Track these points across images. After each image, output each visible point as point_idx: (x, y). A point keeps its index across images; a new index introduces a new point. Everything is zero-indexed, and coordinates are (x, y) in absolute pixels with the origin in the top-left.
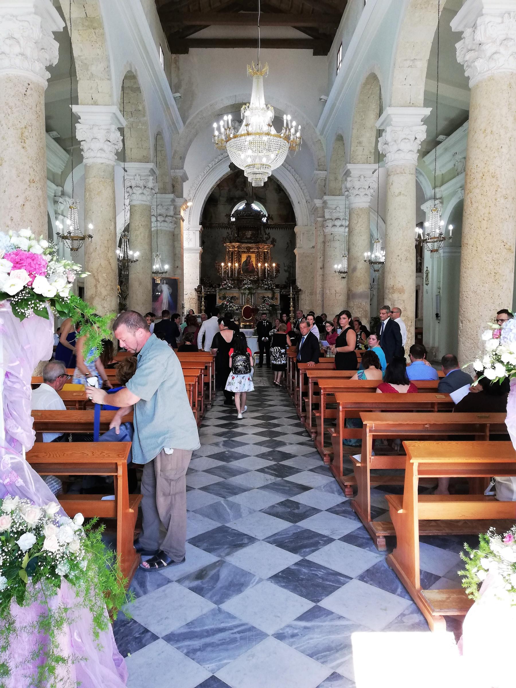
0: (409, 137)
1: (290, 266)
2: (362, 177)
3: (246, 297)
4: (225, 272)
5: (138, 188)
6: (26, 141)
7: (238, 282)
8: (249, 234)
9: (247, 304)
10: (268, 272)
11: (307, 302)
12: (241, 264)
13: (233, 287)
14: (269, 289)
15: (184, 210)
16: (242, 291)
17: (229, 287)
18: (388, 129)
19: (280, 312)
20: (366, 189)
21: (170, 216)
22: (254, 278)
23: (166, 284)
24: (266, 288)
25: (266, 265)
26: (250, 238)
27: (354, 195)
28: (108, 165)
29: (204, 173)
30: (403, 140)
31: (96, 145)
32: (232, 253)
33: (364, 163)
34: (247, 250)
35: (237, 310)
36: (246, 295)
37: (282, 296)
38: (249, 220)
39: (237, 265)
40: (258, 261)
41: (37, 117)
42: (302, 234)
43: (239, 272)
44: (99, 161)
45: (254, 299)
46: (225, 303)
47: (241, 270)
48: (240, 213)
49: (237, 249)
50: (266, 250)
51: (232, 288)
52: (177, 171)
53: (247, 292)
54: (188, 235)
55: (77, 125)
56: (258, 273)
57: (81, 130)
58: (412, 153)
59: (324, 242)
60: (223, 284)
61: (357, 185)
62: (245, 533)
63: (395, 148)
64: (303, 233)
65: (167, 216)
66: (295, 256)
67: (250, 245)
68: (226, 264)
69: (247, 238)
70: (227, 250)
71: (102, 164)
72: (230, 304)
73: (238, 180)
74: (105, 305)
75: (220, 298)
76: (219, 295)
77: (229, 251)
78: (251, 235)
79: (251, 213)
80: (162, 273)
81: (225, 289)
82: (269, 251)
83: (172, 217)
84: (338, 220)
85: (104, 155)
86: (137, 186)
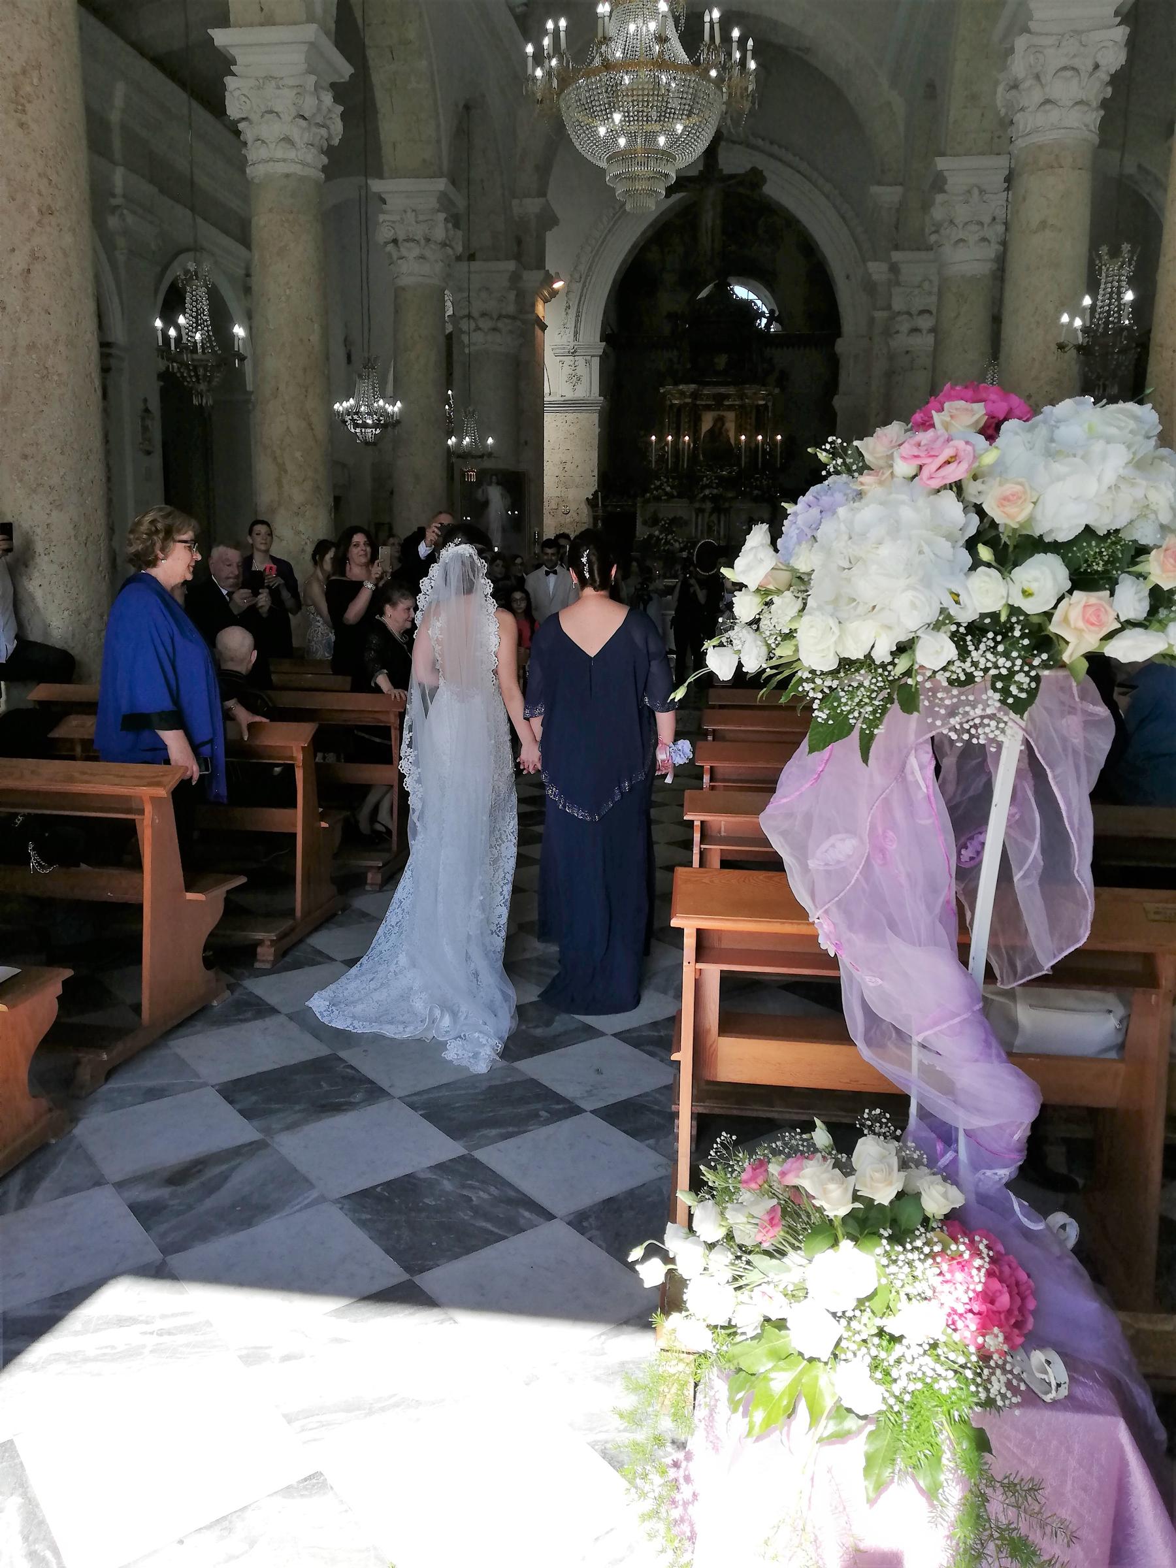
0: (1076, 62)
2: (976, 191)
3: (706, 520)
4: (662, 459)
5: (412, 244)
6: (29, 107)
7: (687, 485)
8: (721, 361)
12: (699, 438)
13: (675, 493)
15: (546, 301)
16: (697, 505)
17: (666, 494)
18: (1020, 43)
20: (986, 226)
21: (508, 316)
22: (730, 473)
23: (498, 484)
27: (952, 242)
28: (302, 179)
29: (614, 208)
30: (1059, 73)
31: (271, 130)
33: (982, 154)
35: (682, 550)
36: (707, 515)
40: (739, 431)
41: (54, 45)
44: (281, 168)
46: (657, 533)
50: (762, 402)
52: (528, 201)
54: (573, 368)
55: (228, 80)
56: (739, 457)
57: (236, 93)
58: (1086, 108)
59: (890, 374)
60: (653, 486)
61: (961, 213)
62: (372, 1076)
63: (1037, 96)
65: (500, 317)
66: (835, 414)
67: (722, 390)
68: (661, 438)
70: (668, 403)
71: (287, 176)
72: (666, 535)
74: (301, 528)
77: (672, 405)
80: (482, 457)
81: (658, 499)
82: (770, 404)
83: (514, 318)
84: (926, 316)
85: (292, 154)
86: (408, 240)
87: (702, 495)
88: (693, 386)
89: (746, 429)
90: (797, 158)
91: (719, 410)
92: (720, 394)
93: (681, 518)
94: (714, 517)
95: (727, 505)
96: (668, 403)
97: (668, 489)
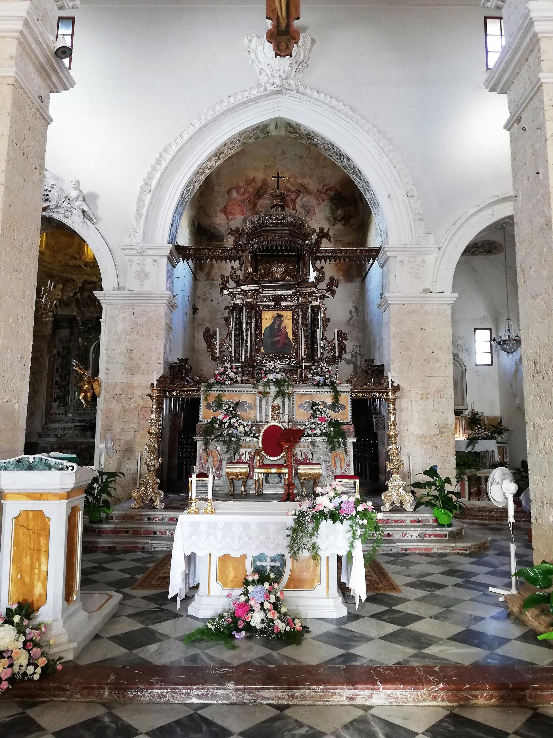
1: (356, 353)
3: (270, 404)
8: (278, 270)
9: (275, 420)
10: (320, 351)
11: (416, 416)
13: (239, 379)
14: (325, 385)
16: (261, 389)
17: (230, 379)
19: (354, 439)
22: (289, 363)
24: (319, 382)
35: (247, 434)
36: (271, 399)
45: (289, 407)
48: (260, 219)
50: (315, 304)
53: (273, 389)
60: (217, 372)
67: (279, 292)
72: (230, 419)
73: (261, 202)
75: (208, 406)
76: (206, 400)
79: (284, 218)
81: (222, 384)
87: (265, 380)
90: (341, 104)
93: (246, 402)
94: (278, 401)
95: (291, 389)
97: (232, 374)
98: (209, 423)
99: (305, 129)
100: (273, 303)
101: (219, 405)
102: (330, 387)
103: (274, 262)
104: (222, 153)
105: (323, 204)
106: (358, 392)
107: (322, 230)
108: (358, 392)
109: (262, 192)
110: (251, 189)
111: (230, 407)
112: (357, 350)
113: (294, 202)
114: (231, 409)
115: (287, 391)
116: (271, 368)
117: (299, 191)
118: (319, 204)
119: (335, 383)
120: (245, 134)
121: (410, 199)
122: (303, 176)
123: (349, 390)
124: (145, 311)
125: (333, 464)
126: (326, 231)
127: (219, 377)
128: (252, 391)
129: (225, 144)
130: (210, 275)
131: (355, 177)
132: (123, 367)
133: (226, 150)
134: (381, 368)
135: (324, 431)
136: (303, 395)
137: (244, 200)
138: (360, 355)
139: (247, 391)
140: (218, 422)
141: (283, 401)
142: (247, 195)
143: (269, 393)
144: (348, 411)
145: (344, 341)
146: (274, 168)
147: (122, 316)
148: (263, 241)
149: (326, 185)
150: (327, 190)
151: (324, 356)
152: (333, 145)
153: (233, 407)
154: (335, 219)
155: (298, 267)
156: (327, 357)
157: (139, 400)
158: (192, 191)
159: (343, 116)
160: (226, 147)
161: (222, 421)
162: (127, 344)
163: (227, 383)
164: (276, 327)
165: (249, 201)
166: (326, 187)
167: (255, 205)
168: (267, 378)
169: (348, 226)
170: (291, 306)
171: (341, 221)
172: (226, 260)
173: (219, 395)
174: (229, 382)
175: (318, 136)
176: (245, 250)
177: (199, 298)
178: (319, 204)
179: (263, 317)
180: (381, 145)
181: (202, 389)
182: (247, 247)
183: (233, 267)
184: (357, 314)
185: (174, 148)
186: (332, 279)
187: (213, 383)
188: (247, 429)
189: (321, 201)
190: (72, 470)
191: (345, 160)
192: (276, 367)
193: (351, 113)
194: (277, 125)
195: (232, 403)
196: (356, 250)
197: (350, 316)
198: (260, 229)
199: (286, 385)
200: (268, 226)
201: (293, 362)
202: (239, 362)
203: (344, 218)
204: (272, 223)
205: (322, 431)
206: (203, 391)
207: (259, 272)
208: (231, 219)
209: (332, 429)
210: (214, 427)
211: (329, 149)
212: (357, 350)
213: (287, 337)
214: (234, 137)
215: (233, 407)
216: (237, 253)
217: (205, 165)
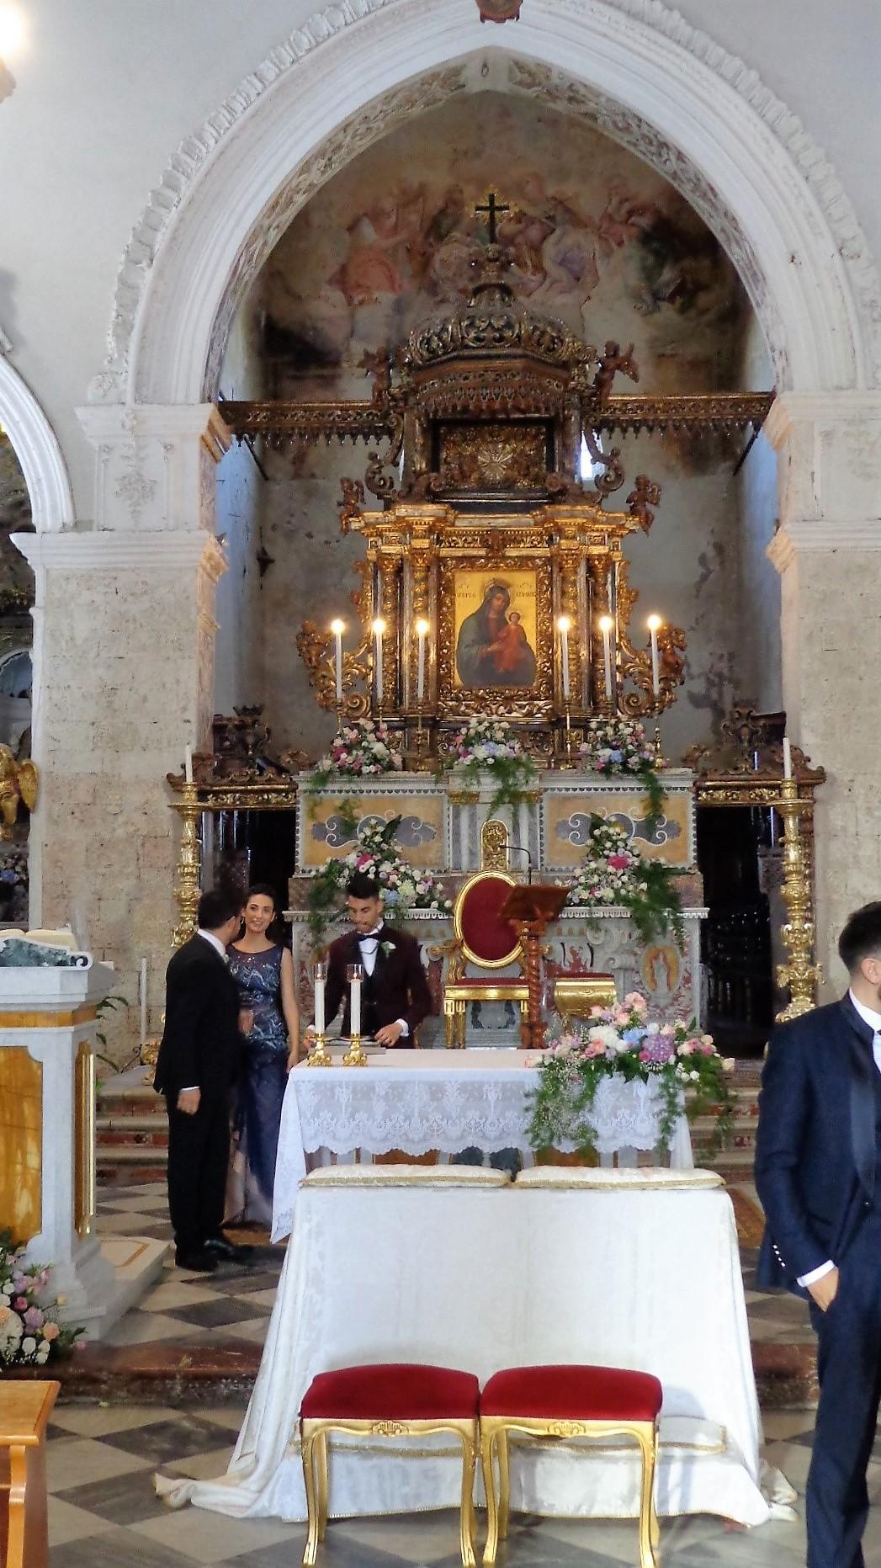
1: (720, 675)
3: (481, 824)
10: (613, 676)
12: (450, 633)
13: (397, 760)
14: (626, 769)
16: (456, 785)
17: (375, 760)
19: (704, 912)
22: (530, 714)
24: (610, 763)
25: (606, 624)
26: (508, 485)
29: (231, 110)
32: (399, 571)
34: (490, 547)
35: (421, 902)
36: (482, 810)
37: (708, 818)
38: (498, 363)
39: (423, 627)
40: (549, 609)
42: (818, 441)
43: (440, 679)
45: (531, 831)
46: (352, 859)
47: (449, 675)
48: (444, 329)
49: (424, 543)
50: (596, 550)
51: (391, 767)
53: (488, 785)
60: (338, 742)
64: (828, 435)
67: (501, 521)
69: (485, 486)
75: (319, 832)
76: (312, 814)
77: (382, 557)
78: (510, 467)
79: (509, 325)
81: (353, 772)
87: (468, 760)
88: (429, 512)
89: (563, 609)
91: (496, 568)
92: (493, 531)
93: (416, 820)
94: (502, 817)
95: (535, 784)
96: (372, 555)
98: (323, 876)
99: (562, 75)
100: (482, 552)
101: (348, 828)
102: (640, 776)
103: (484, 440)
104: (339, 147)
105: (619, 254)
106: (716, 788)
107: (613, 350)
108: (716, 788)
109: (446, 223)
110: (414, 218)
111: (377, 833)
112: (723, 666)
113: (536, 249)
114: (378, 839)
115: (524, 789)
116: (481, 729)
117: (551, 218)
118: (608, 254)
119: (650, 765)
120: (400, 95)
121: (850, 263)
122: (562, 174)
123: (690, 784)
124: (144, 583)
125: (649, 978)
126: (622, 354)
127: (344, 756)
128: (433, 791)
129: (348, 125)
130: (303, 461)
131: (701, 202)
132: (92, 732)
133: (348, 138)
134: (778, 722)
135: (623, 892)
136: (566, 799)
137: (395, 248)
138: (730, 681)
139: (419, 791)
140: (346, 872)
141: (515, 816)
142: (403, 235)
143: (477, 795)
144: (686, 838)
145: (677, 651)
146: (478, 154)
147: (86, 596)
148: (452, 390)
149: (627, 200)
150: (631, 213)
151: (626, 693)
152: (640, 120)
153: (383, 834)
154: (656, 297)
155: (551, 450)
156: (632, 695)
157: (138, 818)
158: (260, 254)
159: (663, 40)
160: (350, 131)
161: (356, 869)
162: (101, 671)
163: (365, 769)
164: (492, 615)
165: (408, 250)
166: (627, 206)
167: (426, 263)
168: (471, 757)
169: (693, 313)
170: (532, 558)
171: (671, 299)
172: (354, 436)
173: (346, 802)
174: (372, 768)
175: (598, 95)
176: (406, 410)
177: (274, 528)
178: (608, 254)
179: (458, 591)
180: (770, 116)
181: (302, 787)
182: (412, 401)
183: (373, 457)
184: (722, 563)
185: (212, 142)
186: (642, 484)
187: (330, 772)
188: (421, 889)
189: (614, 245)
190: (84, 964)
191: (673, 158)
192: (496, 725)
193: (685, 30)
194: (485, 66)
195: (380, 822)
196: (709, 402)
197: (701, 570)
198: (444, 354)
199: (521, 773)
200: (467, 347)
201: (540, 709)
202: (396, 712)
203: (680, 290)
204: (477, 339)
205: (617, 892)
206: (305, 791)
207: (443, 469)
208: (361, 303)
209: (644, 886)
210: (333, 885)
211: (627, 129)
212: (723, 666)
213: (524, 644)
214: (370, 105)
215: (383, 834)
216: (386, 416)
217: (294, 184)
